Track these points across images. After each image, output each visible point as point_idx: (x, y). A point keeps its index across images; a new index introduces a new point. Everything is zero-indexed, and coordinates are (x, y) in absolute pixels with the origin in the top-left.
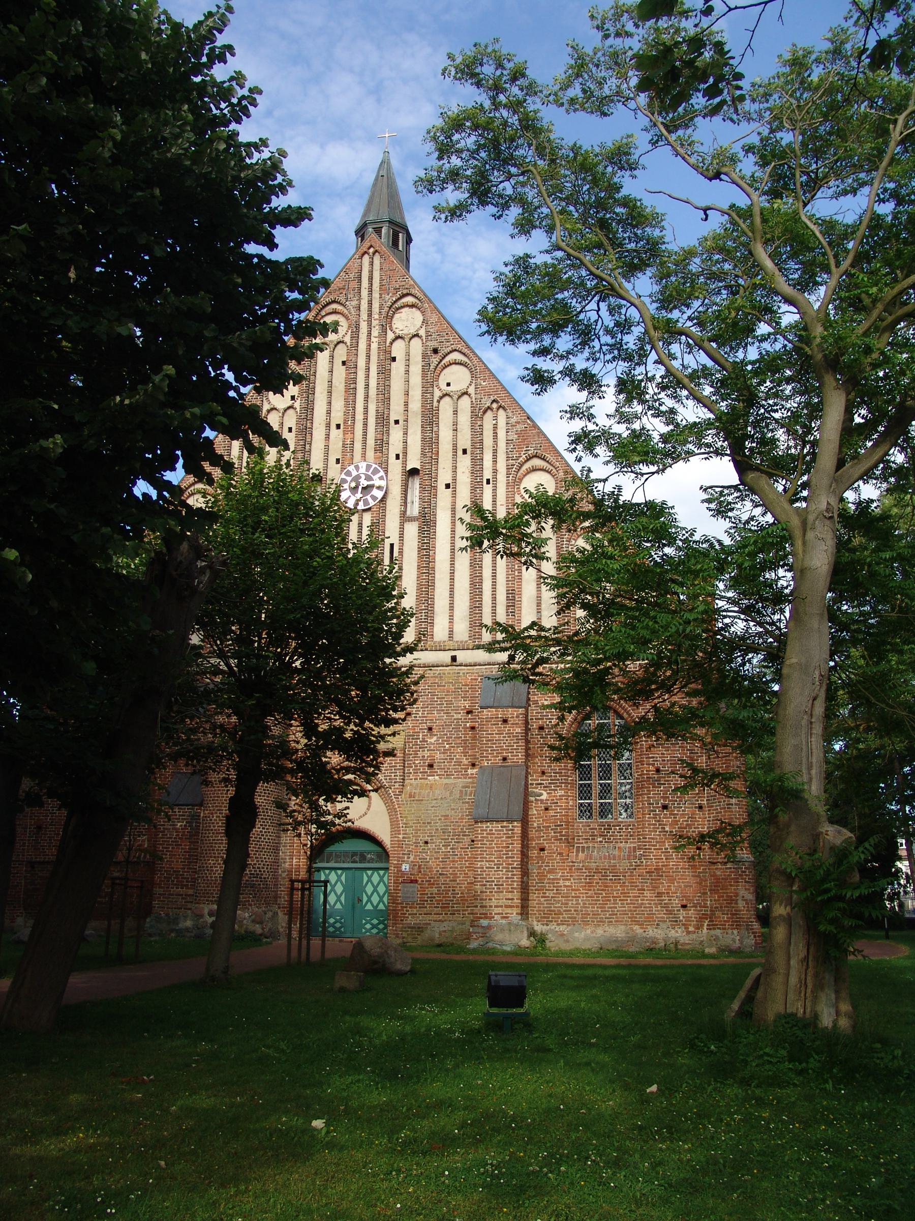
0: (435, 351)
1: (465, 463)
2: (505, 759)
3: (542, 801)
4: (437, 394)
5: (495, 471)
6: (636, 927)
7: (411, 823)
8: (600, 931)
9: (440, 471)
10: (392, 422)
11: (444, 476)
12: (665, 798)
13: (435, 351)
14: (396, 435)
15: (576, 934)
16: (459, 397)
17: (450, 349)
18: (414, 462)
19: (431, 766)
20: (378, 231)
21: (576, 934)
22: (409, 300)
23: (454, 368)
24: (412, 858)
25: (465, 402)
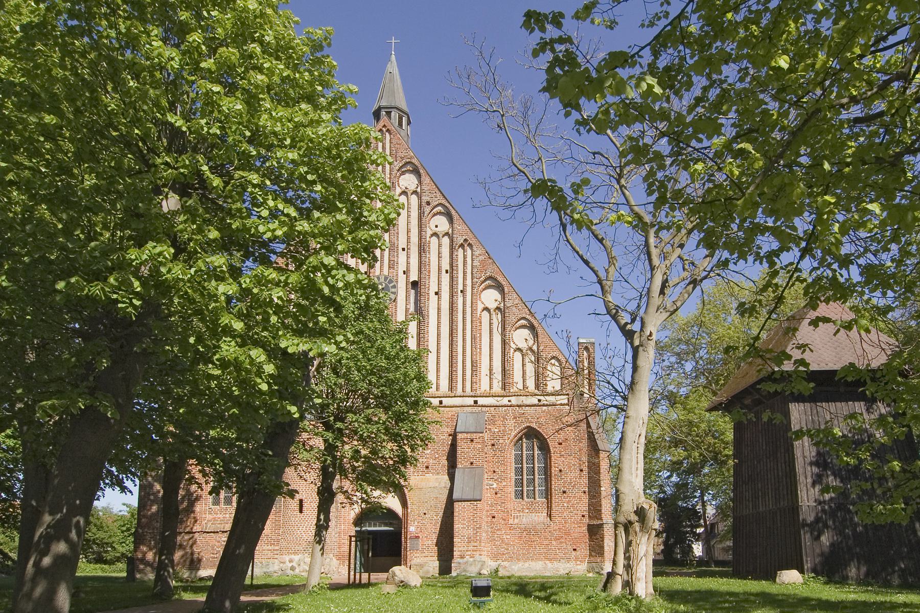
0: (428, 203)
1: (446, 278)
2: (472, 463)
3: (493, 489)
4: (429, 232)
5: (464, 285)
6: (547, 562)
7: (415, 502)
8: (527, 565)
9: (431, 284)
10: (400, 249)
11: (434, 288)
12: (564, 487)
13: (428, 203)
14: (402, 258)
15: (513, 567)
16: (443, 236)
17: (437, 203)
18: (414, 277)
19: (427, 467)
20: (389, 114)
21: (513, 567)
22: (409, 167)
23: (438, 217)
24: (416, 524)
25: (446, 241)
